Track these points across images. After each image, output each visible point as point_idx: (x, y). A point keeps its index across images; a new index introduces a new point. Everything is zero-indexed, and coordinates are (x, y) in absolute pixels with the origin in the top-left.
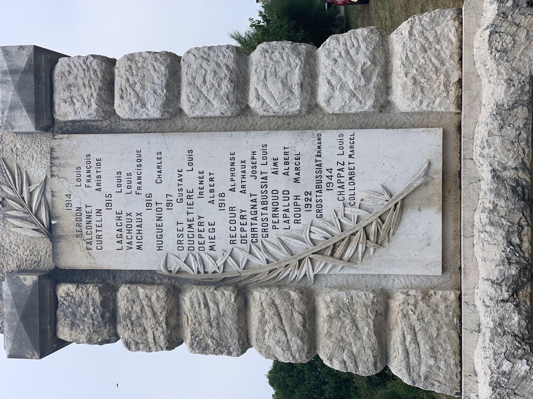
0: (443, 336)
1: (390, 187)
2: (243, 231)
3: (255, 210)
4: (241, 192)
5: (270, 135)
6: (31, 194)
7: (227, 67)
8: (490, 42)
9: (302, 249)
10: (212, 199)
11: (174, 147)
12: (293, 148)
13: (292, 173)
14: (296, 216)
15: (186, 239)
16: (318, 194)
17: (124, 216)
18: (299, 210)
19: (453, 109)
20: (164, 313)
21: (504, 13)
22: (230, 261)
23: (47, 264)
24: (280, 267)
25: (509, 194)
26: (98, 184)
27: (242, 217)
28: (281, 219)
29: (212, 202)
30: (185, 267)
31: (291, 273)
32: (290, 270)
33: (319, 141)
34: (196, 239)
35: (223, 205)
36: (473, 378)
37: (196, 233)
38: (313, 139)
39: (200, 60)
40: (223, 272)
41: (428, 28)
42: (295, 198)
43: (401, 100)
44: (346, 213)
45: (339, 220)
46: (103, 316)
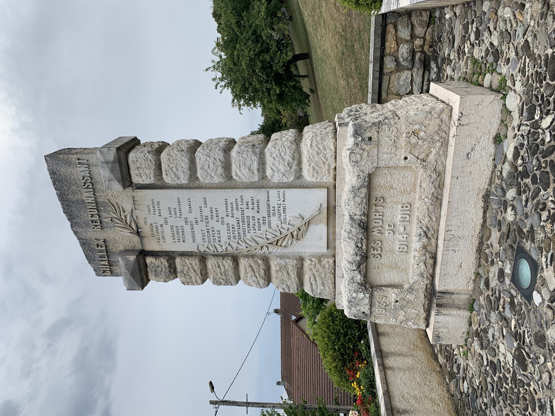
1: (303, 215)
6: (126, 216)
7: (220, 160)
8: (350, 158)
11: (197, 195)
13: (256, 208)
15: (206, 237)
17: (174, 228)
19: (332, 181)
20: (199, 270)
21: (357, 144)
23: (139, 247)
25: (357, 227)
26: (160, 213)
27: (233, 228)
30: (208, 250)
34: (212, 238)
36: (340, 295)
37: (211, 235)
39: (205, 157)
41: (320, 143)
43: (307, 175)
46: (170, 272)
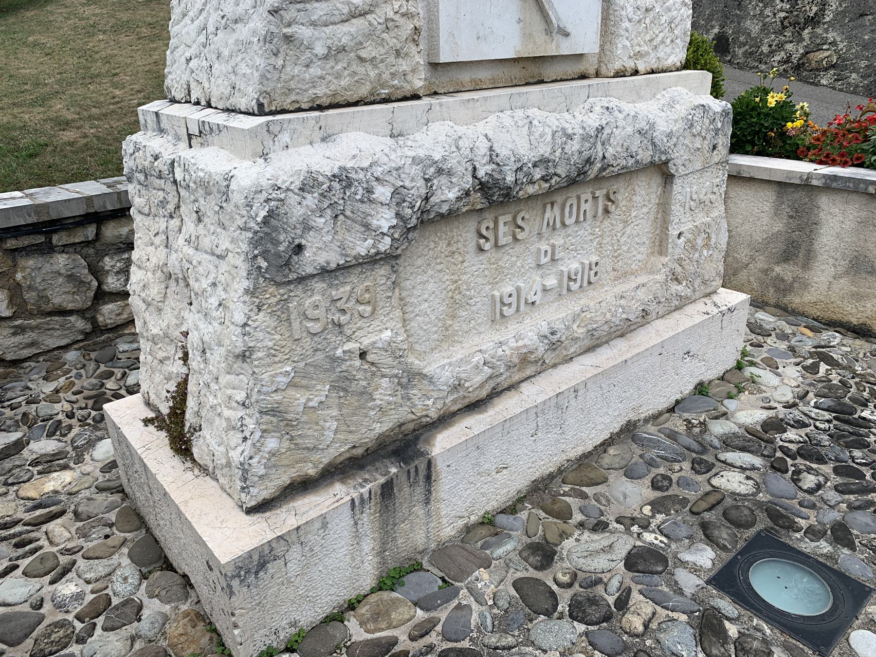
0: (361, 70)
19: (617, 65)
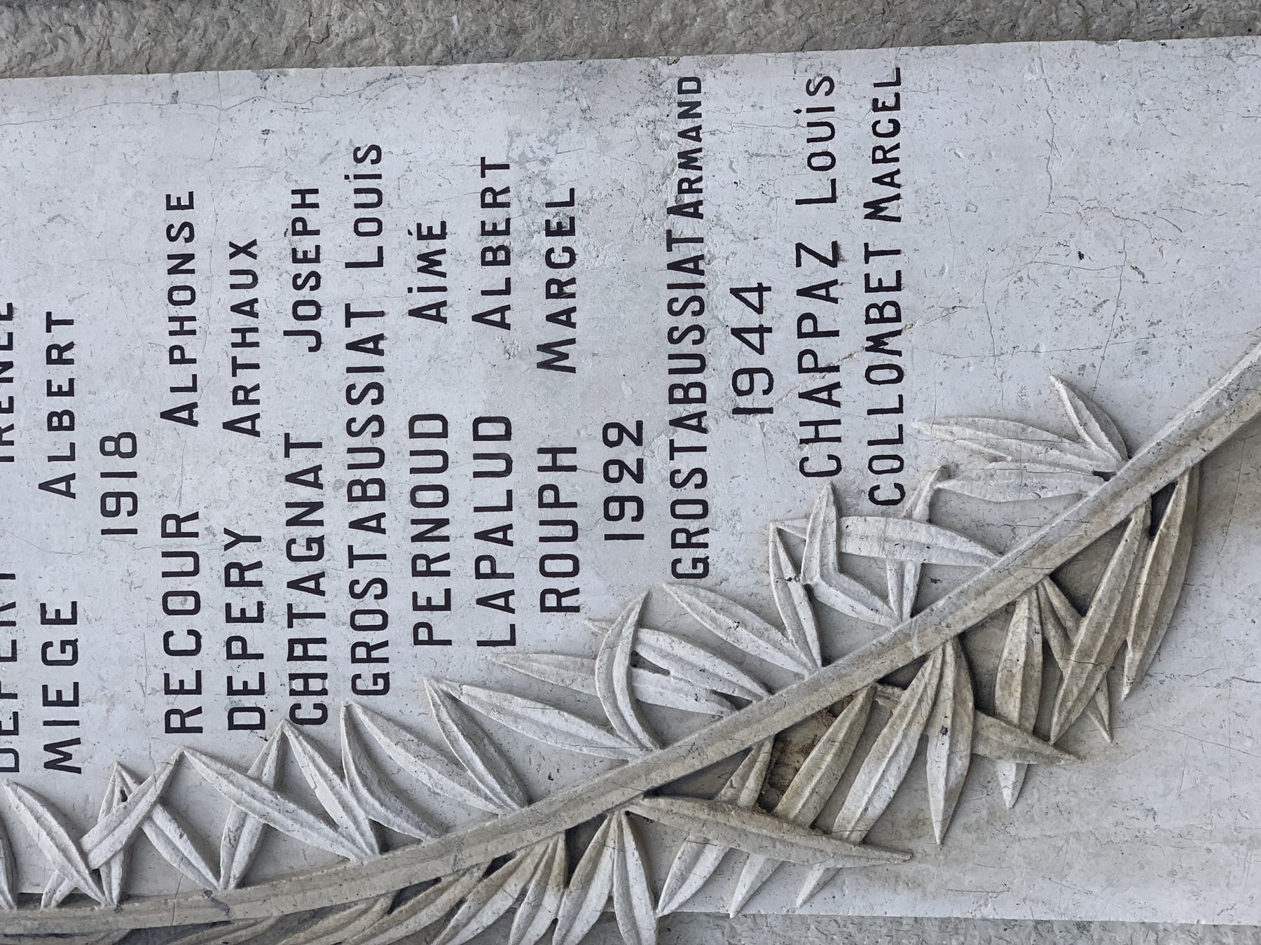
1: (1122, 392)
2: (245, 655)
3: (316, 532)
4: (230, 425)
5: (397, 93)
9: (587, 761)
10: (64, 469)
12: (534, 167)
13: (530, 313)
14: (551, 566)
16: (684, 437)
18: (567, 531)
22: (160, 832)
24: (459, 874)
27: (238, 575)
28: (466, 587)
29: (61, 487)
31: (523, 910)
32: (513, 887)
33: (687, 124)
35: (126, 503)
38: (651, 112)
40: (125, 897)
42: (547, 460)
44: (850, 547)
45: (809, 590)
